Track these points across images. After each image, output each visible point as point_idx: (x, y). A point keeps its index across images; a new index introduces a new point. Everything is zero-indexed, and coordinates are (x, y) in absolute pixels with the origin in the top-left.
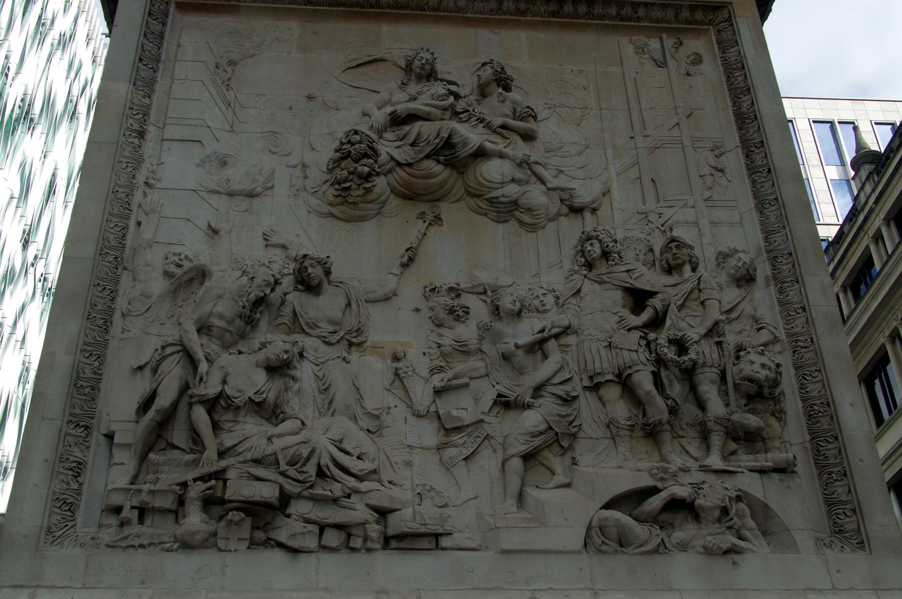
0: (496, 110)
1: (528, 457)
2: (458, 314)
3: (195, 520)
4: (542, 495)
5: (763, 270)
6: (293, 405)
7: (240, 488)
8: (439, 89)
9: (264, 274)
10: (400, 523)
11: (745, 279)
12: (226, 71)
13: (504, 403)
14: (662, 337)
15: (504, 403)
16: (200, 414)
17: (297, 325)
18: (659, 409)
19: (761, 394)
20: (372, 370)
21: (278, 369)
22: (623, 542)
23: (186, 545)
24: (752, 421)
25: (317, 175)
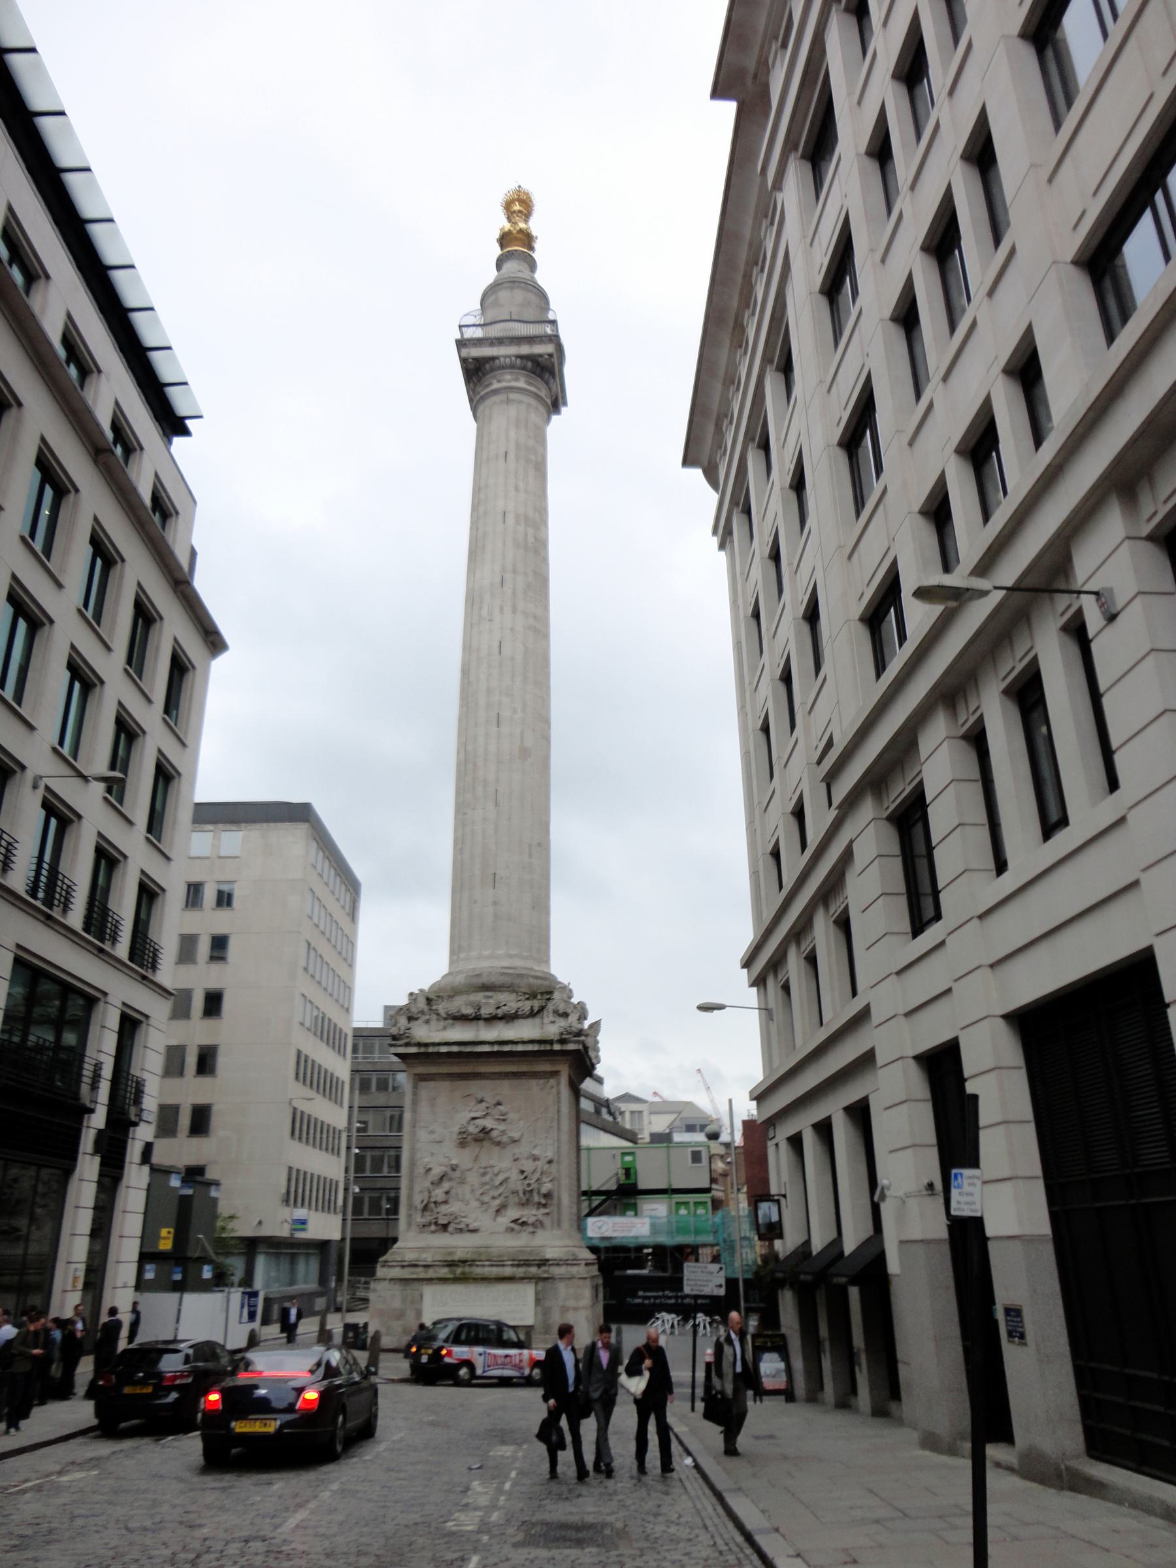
0: (495, 1112)
1: (498, 1211)
2: (484, 1174)
3: (433, 1228)
4: (500, 1219)
5: (556, 1159)
6: (451, 1201)
7: (441, 1221)
8: (484, 1105)
9: (444, 1169)
10: (471, 1227)
11: (550, 1162)
12: (432, 1101)
13: (494, 1198)
14: (527, 1182)
15: (494, 1198)
16: (432, 1205)
17: (450, 1180)
18: (524, 1199)
19: (548, 1196)
20: (467, 1189)
21: (447, 1193)
22: (512, 1230)
23: (433, 1232)
24: (543, 1201)
25: (455, 1136)
